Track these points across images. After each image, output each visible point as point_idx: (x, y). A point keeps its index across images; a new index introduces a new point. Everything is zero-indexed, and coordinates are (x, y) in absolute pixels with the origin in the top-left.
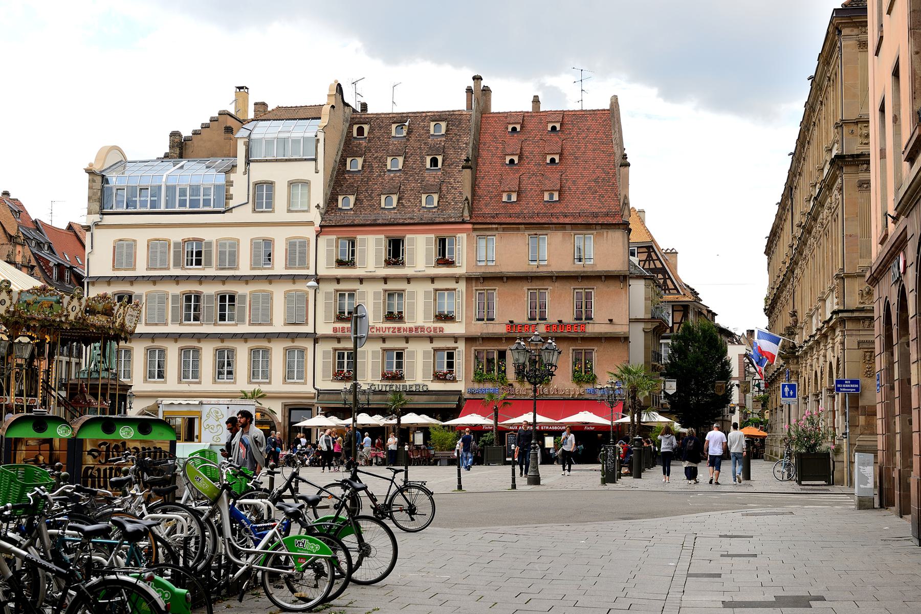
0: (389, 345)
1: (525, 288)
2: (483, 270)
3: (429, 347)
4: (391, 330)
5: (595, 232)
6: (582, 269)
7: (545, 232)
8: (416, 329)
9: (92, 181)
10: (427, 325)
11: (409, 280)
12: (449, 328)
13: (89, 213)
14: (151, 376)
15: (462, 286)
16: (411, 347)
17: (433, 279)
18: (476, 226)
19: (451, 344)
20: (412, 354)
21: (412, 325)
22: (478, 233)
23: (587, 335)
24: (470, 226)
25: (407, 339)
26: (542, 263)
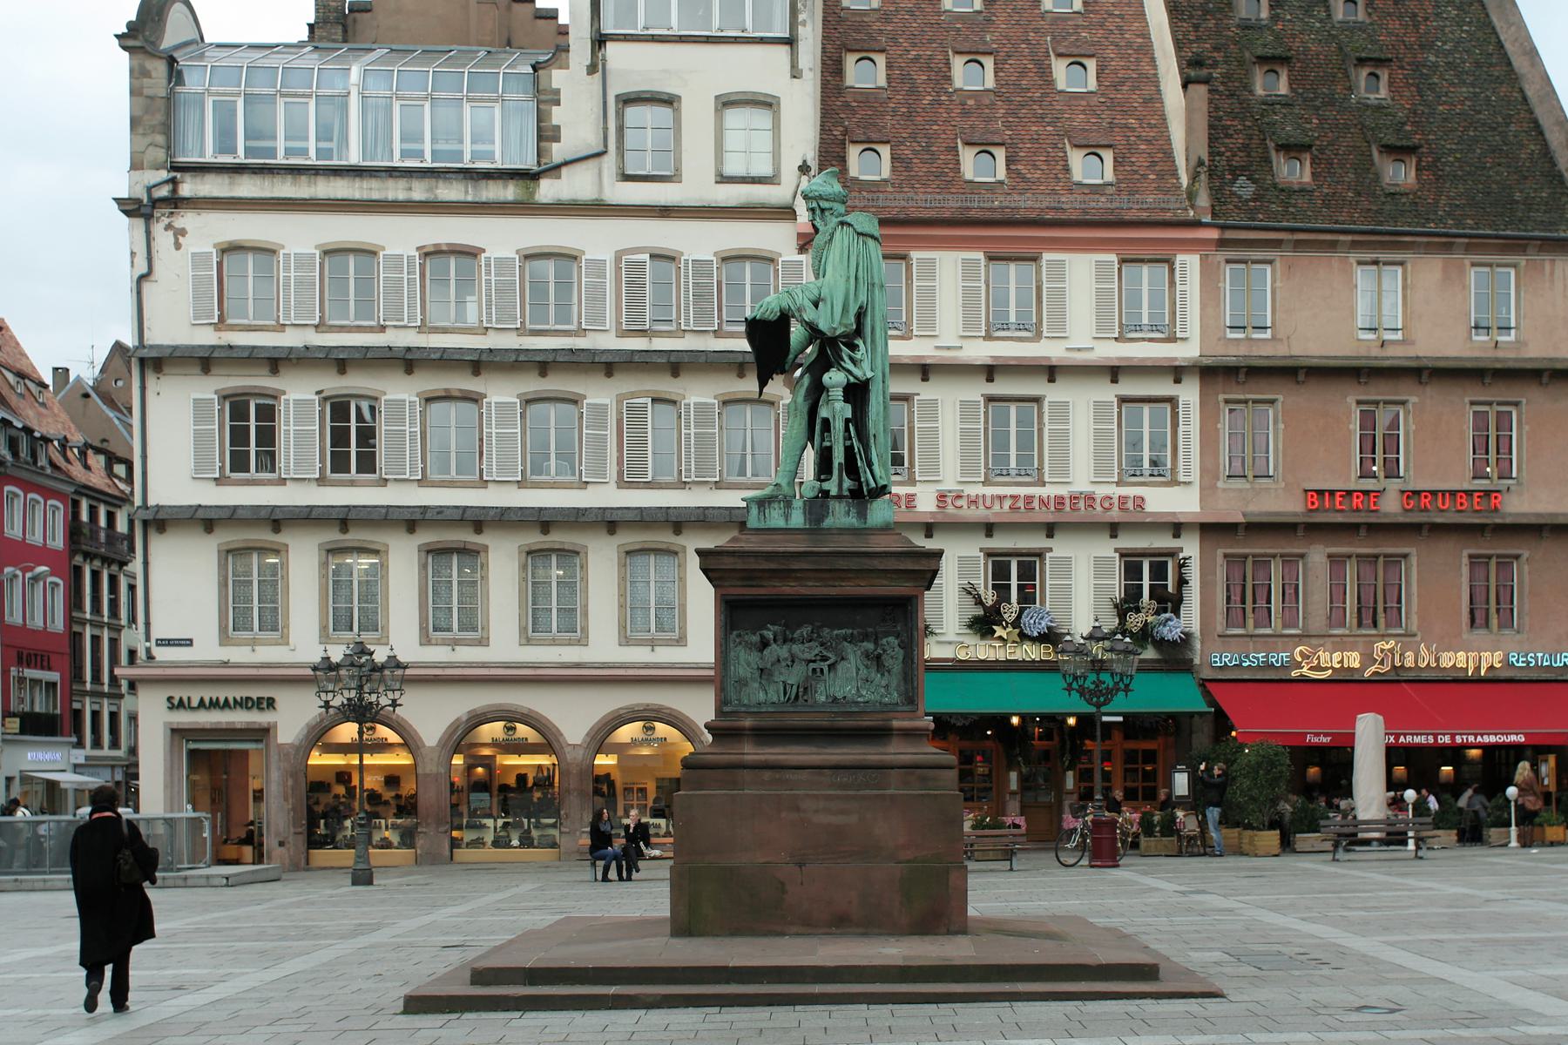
0: (1000, 542)
1: (1351, 400)
2: (1242, 350)
3: (1106, 548)
4: (1007, 504)
5: (1522, 260)
6: (1491, 354)
7: (1398, 257)
8: (1074, 498)
9: (137, 74)
10: (1101, 491)
11: (1052, 372)
12: (1163, 501)
13: (136, 165)
14: (242, 623)
15: (1189, 394)
16: (1060, 548)
17: (1114, 372)
18: (1230, 235)
19: (1164, 542)
20: (1065, 565)
21: (1063, 491)
22: (1232, 254)
23: (1508, 520)
24: (1214, 234)
25: (1050, 530)
26: (1388, 336)
